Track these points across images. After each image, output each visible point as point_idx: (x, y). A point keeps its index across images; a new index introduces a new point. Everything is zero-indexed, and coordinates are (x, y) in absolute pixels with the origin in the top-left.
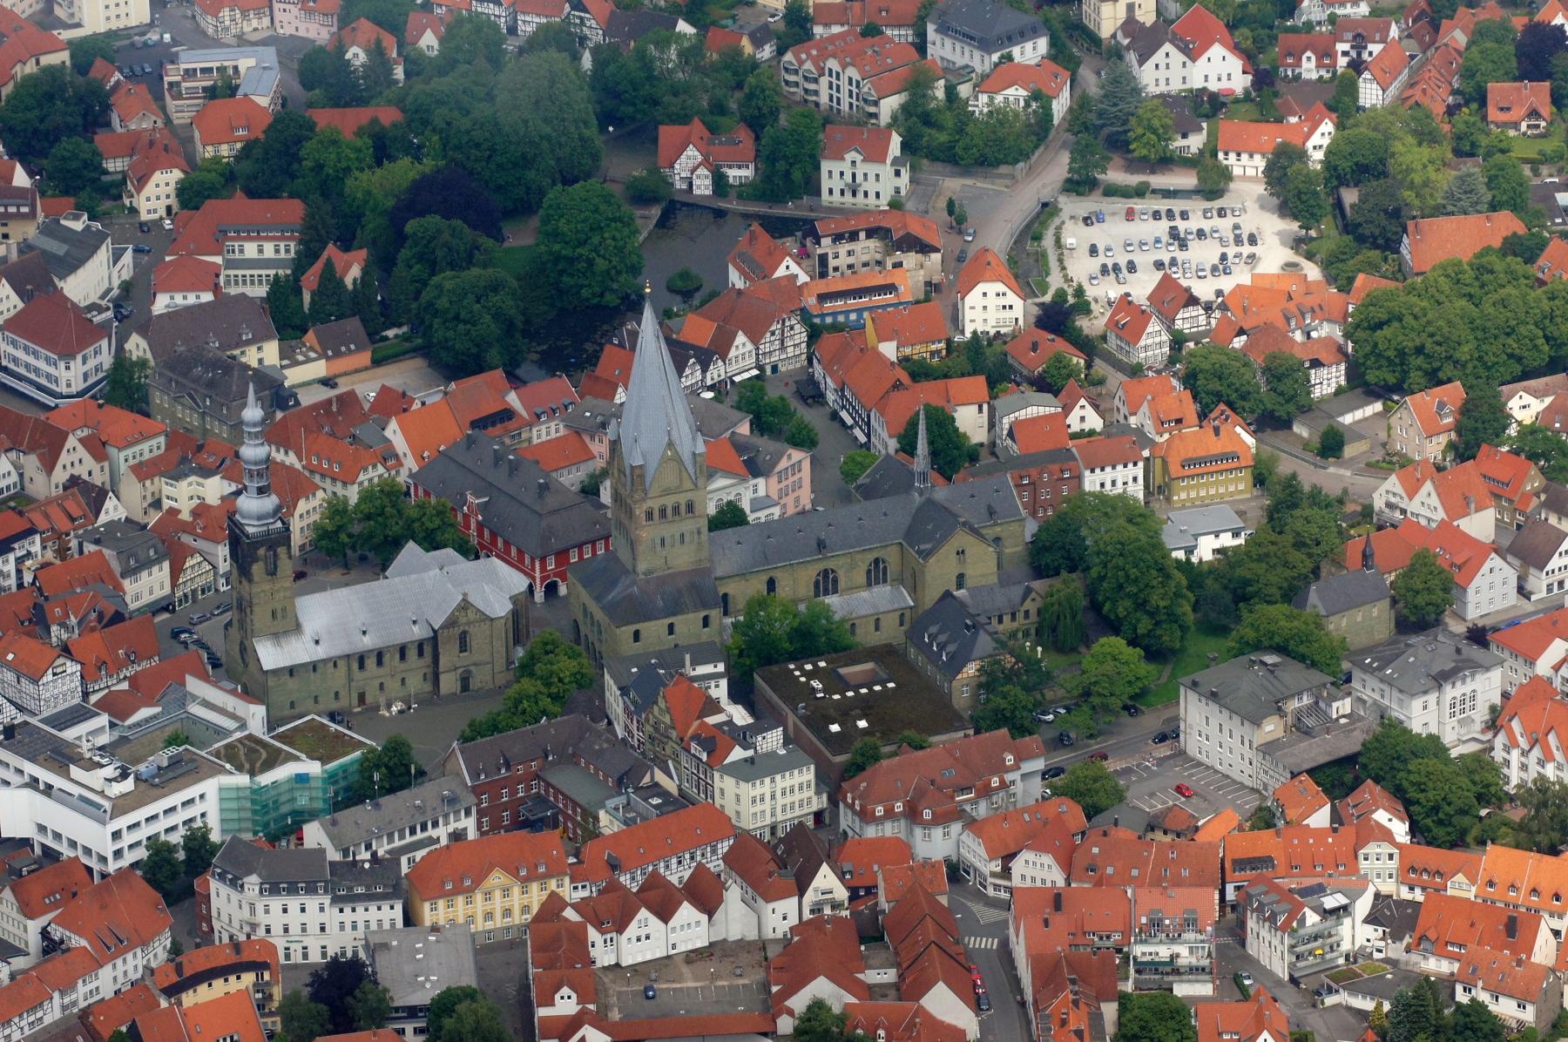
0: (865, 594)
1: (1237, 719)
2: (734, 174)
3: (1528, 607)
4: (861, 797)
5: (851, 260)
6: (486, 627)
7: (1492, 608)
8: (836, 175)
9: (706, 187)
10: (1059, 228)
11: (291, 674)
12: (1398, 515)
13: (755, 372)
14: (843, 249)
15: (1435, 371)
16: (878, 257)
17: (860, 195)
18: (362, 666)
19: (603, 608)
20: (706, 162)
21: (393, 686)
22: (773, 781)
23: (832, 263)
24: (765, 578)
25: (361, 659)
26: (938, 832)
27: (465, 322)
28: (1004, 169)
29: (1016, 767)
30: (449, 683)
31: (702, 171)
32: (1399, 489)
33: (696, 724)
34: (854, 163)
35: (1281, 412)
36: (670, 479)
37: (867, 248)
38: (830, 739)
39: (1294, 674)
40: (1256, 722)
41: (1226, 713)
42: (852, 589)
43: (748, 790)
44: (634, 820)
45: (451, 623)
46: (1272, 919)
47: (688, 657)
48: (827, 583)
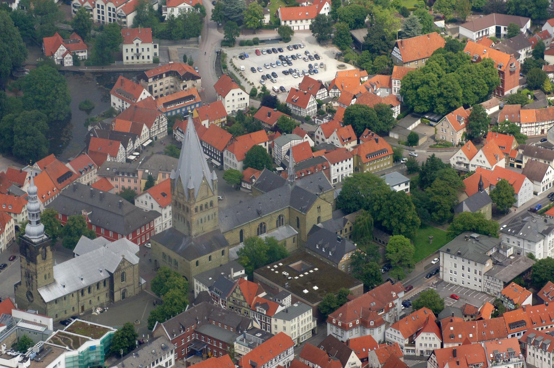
0: (276, 231)
1: (473, 263)
2: (83, 55)
3: (538, 198)
4: (340, 320)
5: (161, 87)
6: (131, 269)
7: (525, 201)
8: (130, 50)
9: (70, 63)
10: (231, 62)
11: (56, 303)
12: (463, 166)
13: (150, 141)
14: (158, 82)
15: (448, 103)
16: (172, 84)
17: (141, 58)
18: (82, 294)
19: (179, 254)
20: (69, 51)
21: (95, 300)
22: (298, 319)
23: (154, 89)
24: (239, 230)
25: (82, 291)
26: (376, 330)
27: (30, 135)
28: (192, 39)
29: (397, 297)
30: (117, 296)
31: (68, 56)
32: (463, 155)
33: (255, 298)
34: (137, 44)
35: (386, 130)
36: (204, 194)
37: (167, 81)
38: (304, 296)
39: (485, 240)
40: (483, 263)
41: (466, 261)
42: (271, 230)
43: (289, 324)
44: (255, 344)
45: (118, 269)
46: (543, 347)
47: (232, 269)
48: (262, 229)
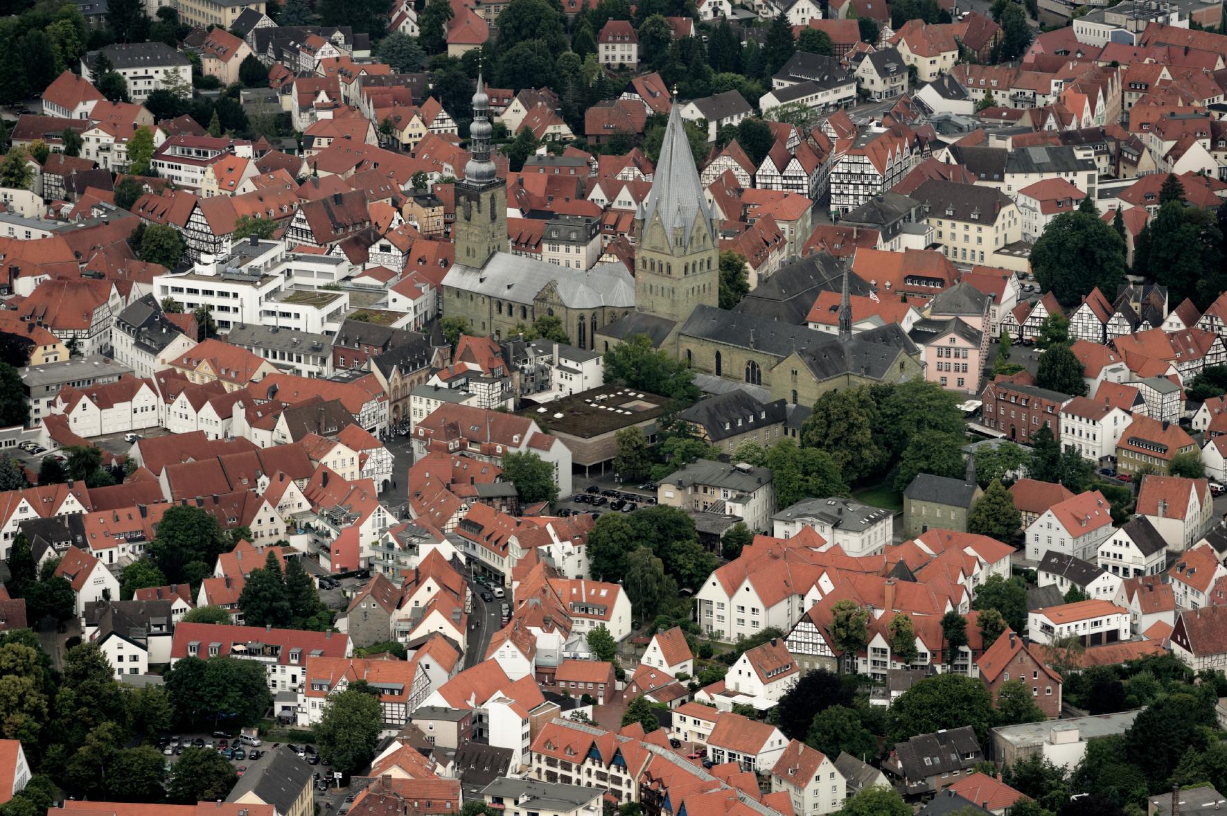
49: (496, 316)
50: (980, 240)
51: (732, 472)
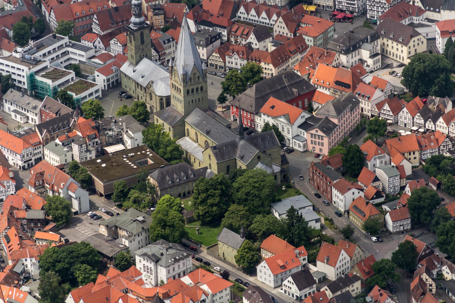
25: (138, 84)
49: (137, 89)
50: (402, 51)
51: (134, 221)
